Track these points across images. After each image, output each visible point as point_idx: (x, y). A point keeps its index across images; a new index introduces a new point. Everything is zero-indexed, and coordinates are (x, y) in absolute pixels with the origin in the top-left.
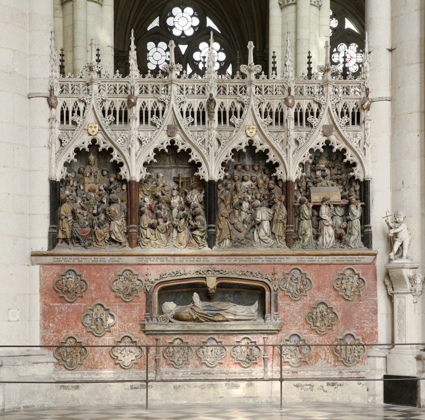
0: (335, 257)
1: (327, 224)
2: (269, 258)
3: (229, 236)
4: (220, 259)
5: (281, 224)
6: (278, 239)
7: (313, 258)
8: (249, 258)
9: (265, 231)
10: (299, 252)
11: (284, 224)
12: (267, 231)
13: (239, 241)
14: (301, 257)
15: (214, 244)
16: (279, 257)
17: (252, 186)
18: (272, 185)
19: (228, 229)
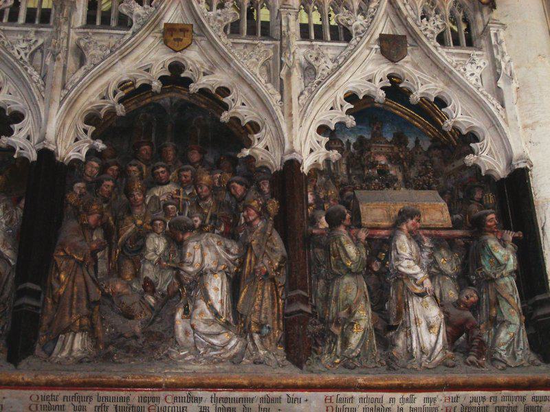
0: (454, 394)
1: (419, 290)
2: (226, 400)
3: (85, 321)
4: (44, 398)
5: (268, 288)
6: (256, 336)
7: (380, 400)
8: (154, 399)
9: (211, 307)
10: (331, 378)
11: (275, 286)
12: (218, 307)
13: (121, 340)
14: (342, 394)
15: (28, 351)
16: (262, 394)
17: (178, 193)
18: (238, 187)
19: (84, 297)
